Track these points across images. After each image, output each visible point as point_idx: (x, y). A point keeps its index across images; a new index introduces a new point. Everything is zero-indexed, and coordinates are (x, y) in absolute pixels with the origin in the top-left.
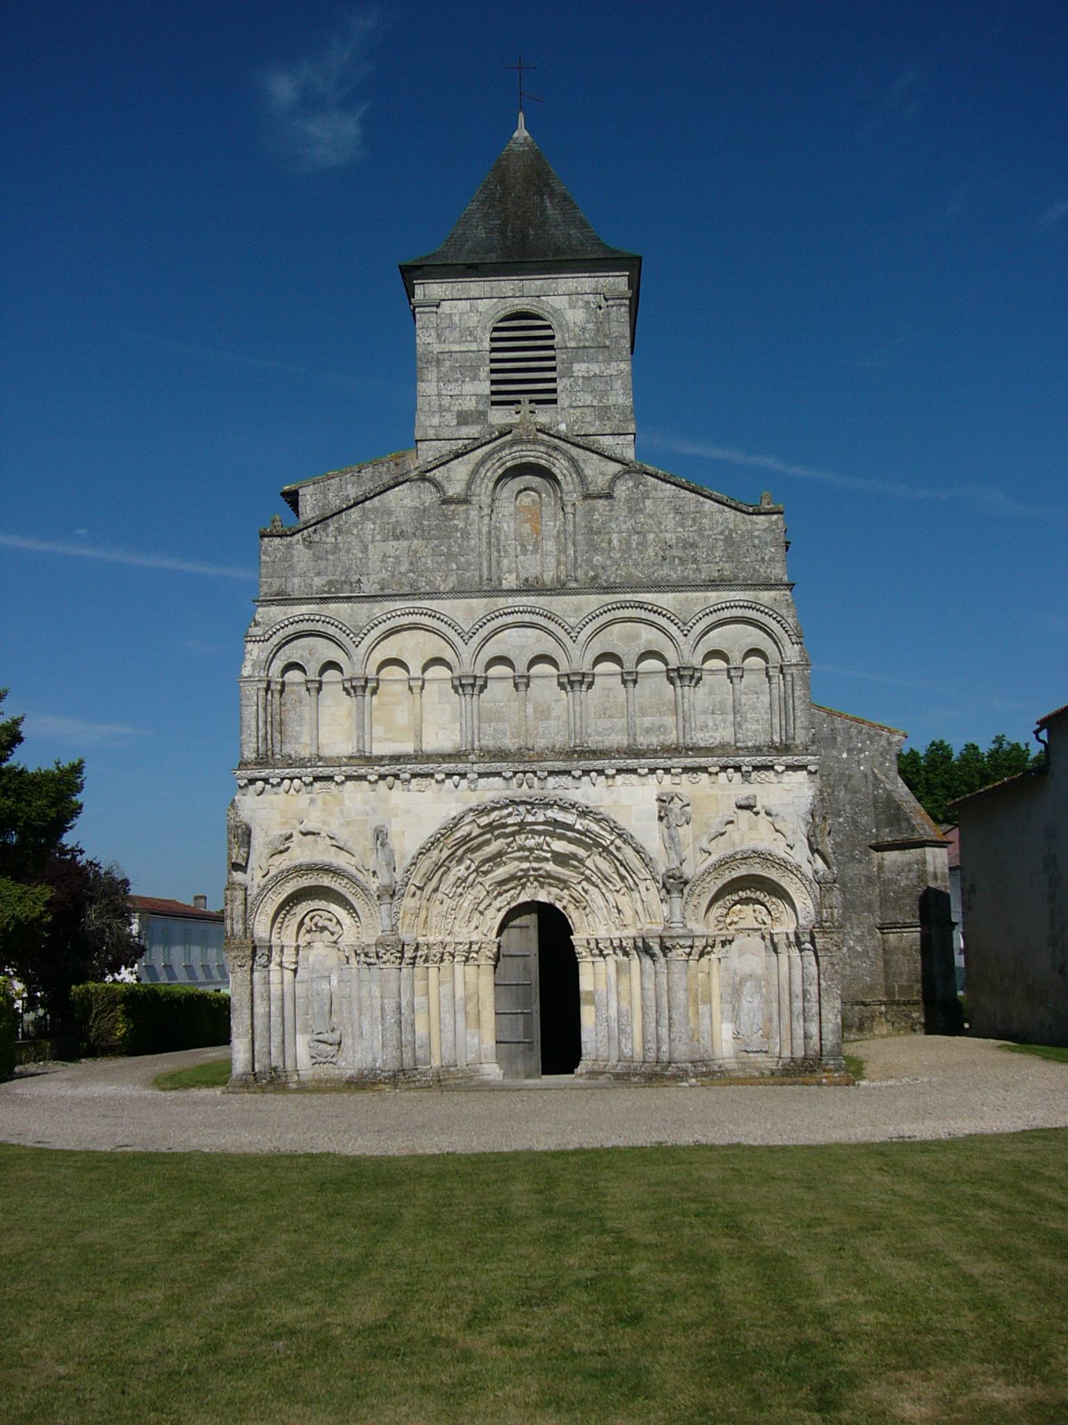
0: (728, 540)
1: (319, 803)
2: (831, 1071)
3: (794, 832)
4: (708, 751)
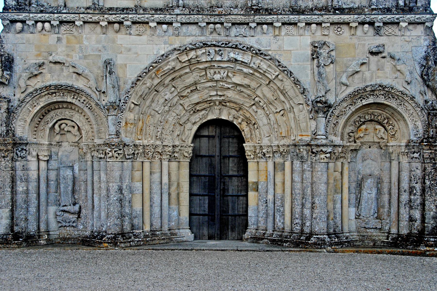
1: (64, 41)
2: (431, 246)
3: (411, 73)
4: (351, 11)
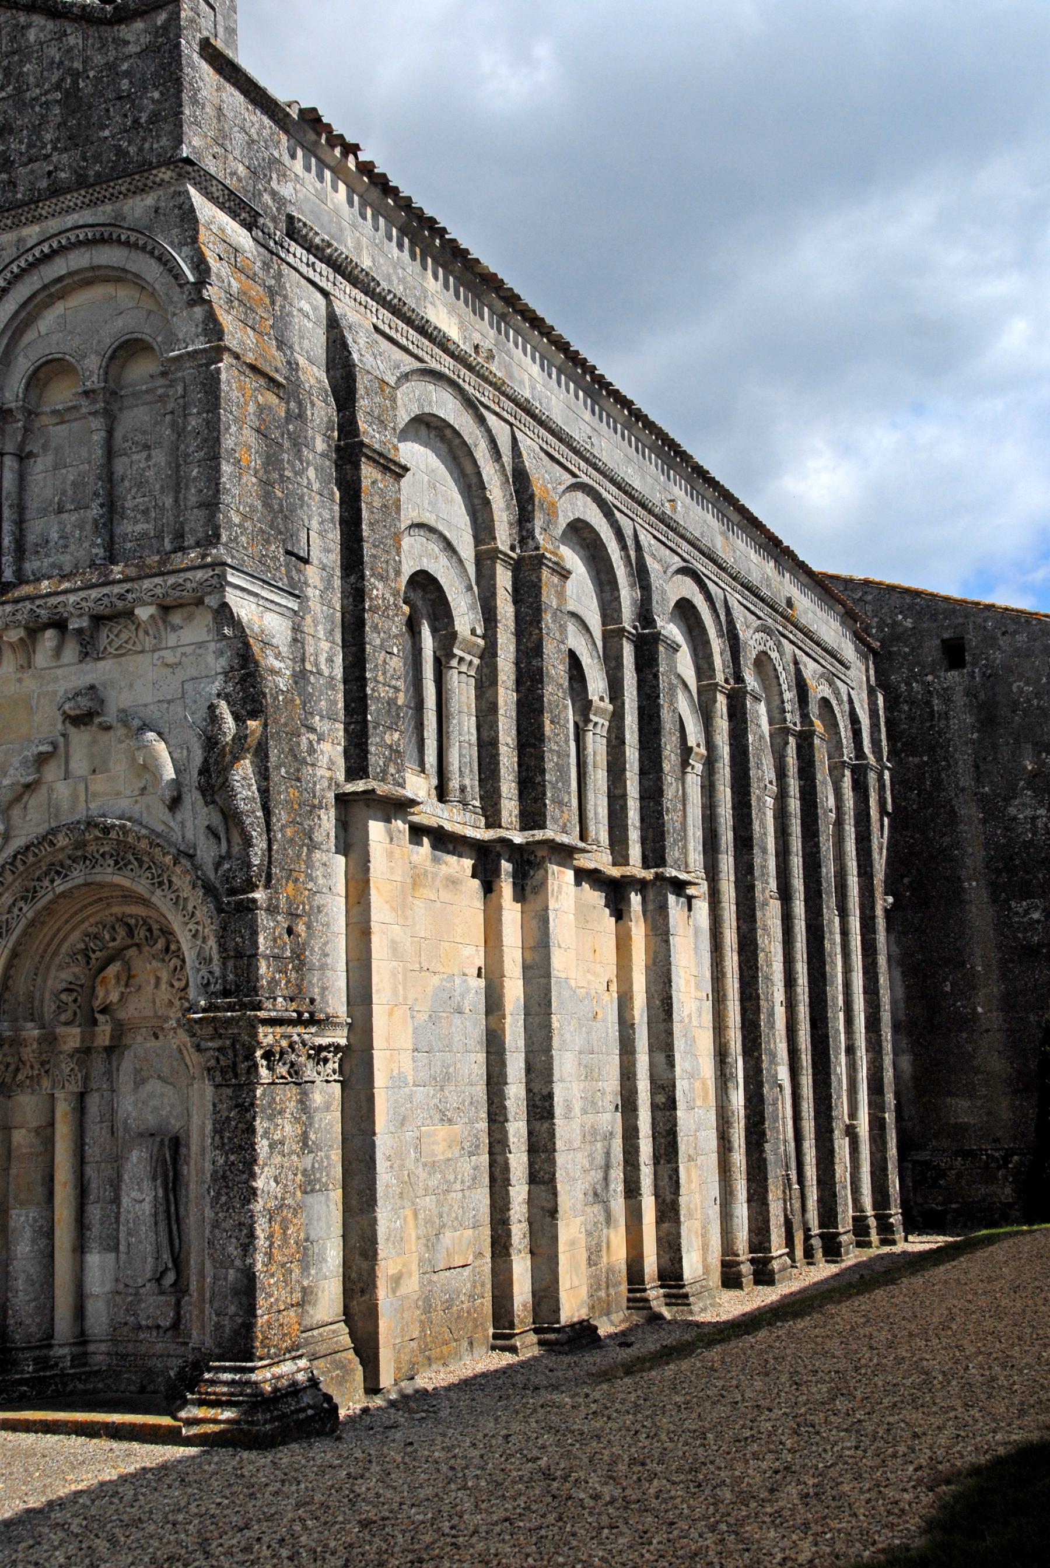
0: (72, 101)
